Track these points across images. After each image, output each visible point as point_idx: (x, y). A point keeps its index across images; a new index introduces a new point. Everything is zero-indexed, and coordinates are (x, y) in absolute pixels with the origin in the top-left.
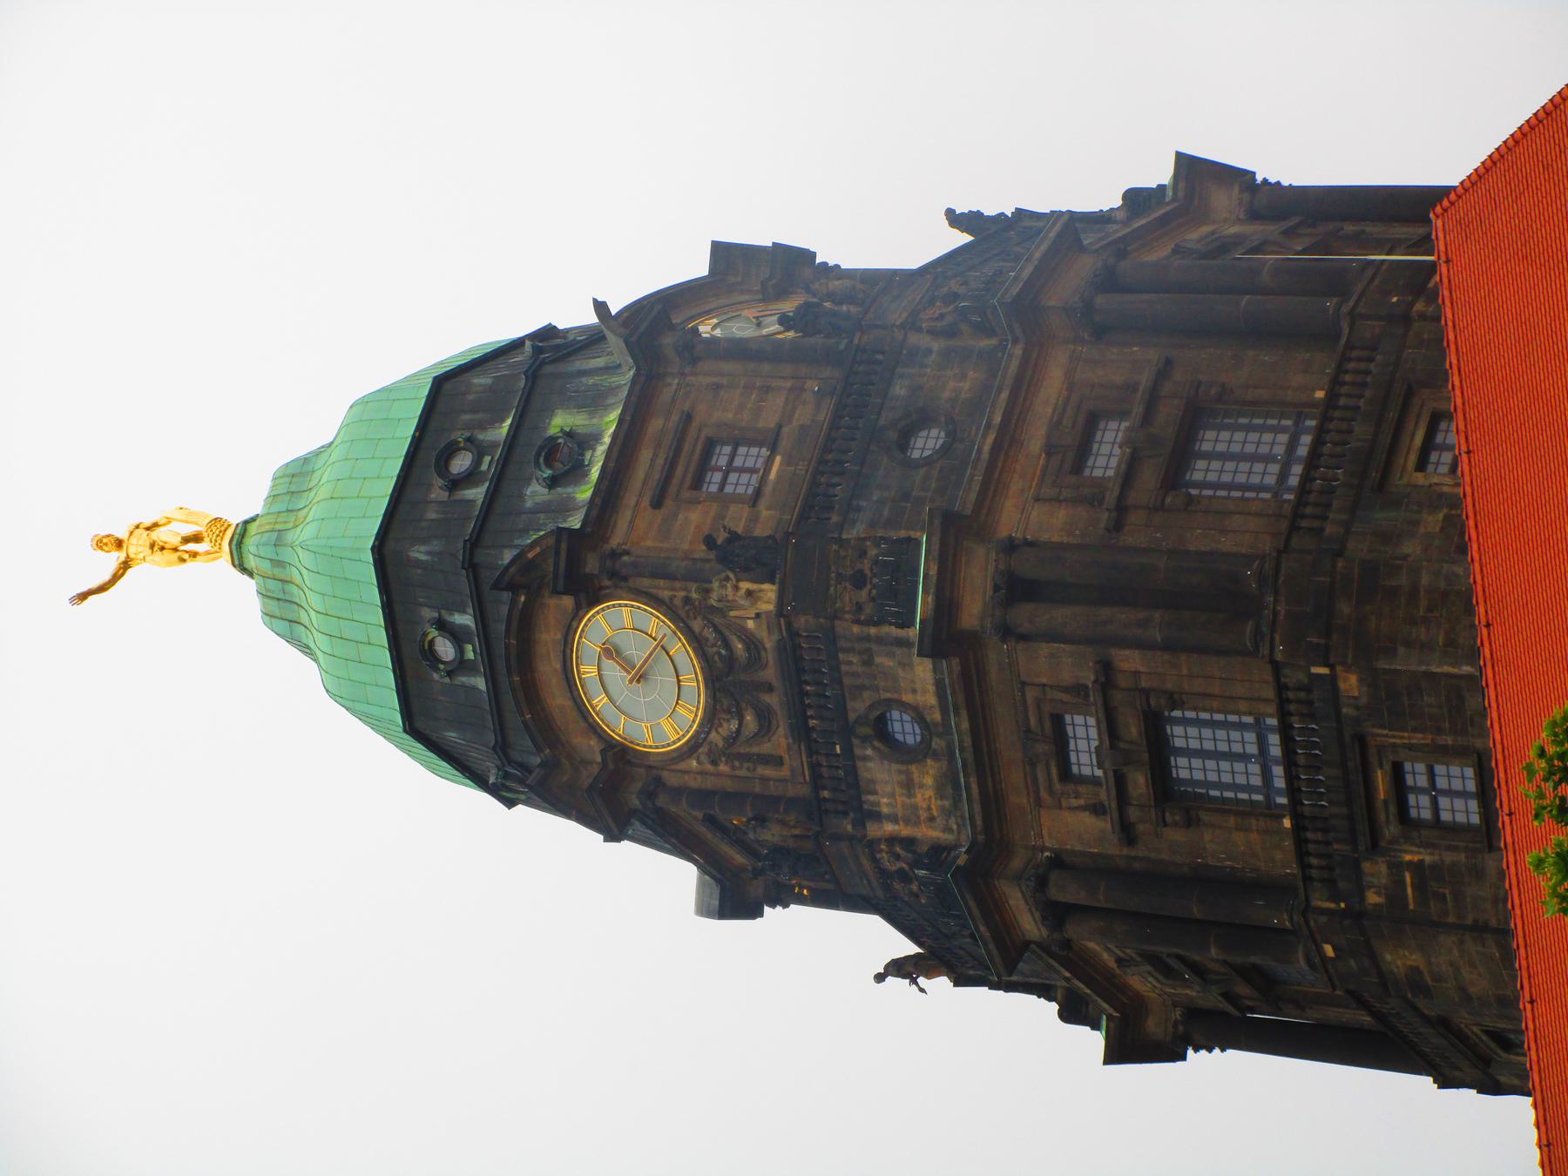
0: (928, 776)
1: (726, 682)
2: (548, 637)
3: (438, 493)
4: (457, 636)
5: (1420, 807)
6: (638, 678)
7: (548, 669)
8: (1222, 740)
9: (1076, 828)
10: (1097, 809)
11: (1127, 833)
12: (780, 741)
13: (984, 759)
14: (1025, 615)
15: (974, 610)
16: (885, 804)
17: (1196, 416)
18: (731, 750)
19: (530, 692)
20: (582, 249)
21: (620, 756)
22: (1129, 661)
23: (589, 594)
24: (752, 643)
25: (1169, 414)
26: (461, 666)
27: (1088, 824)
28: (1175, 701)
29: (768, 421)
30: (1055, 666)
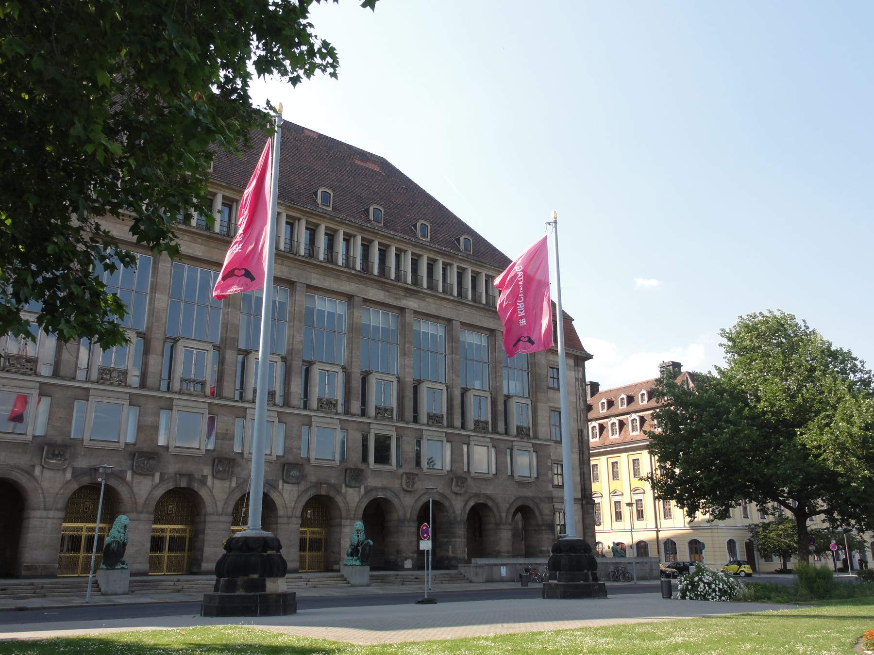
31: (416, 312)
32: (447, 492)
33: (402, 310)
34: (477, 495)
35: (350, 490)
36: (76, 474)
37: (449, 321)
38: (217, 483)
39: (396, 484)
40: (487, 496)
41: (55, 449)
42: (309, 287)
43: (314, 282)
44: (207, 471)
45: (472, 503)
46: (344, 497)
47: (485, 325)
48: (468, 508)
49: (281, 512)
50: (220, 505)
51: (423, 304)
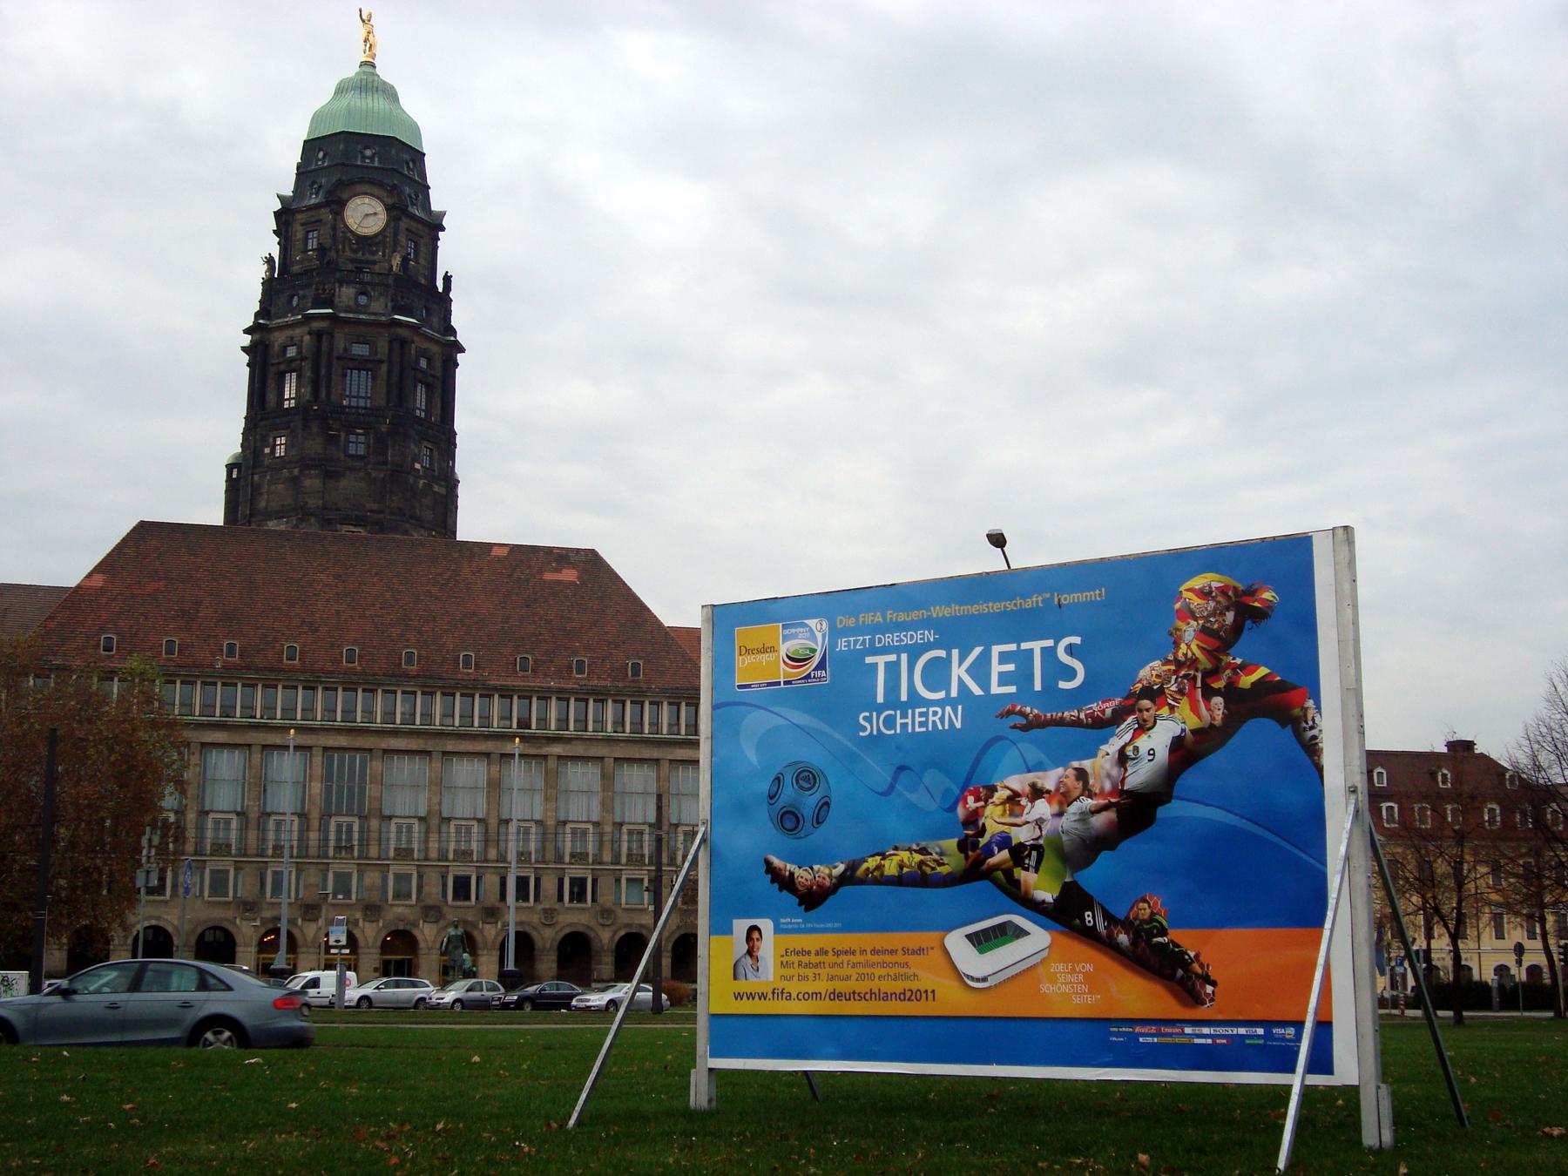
0: (352, 303)
1: (365, 242)
2: (375, 190)
3: (406, 157)
4: (372, 158)
5: (352, 438)
6: (365, 215)
7: (366, 188)
8: (363, 387)
9: (340, 345)
10: (345, 350)
11: (339, 358)
12: (349, 254)
13: (359, 322)
14: (396, 345)
15: (401, 332)
16: (344, 289)
17: (429, 387)
18: (345, 237)
19: (362, 181)
20: (445, 190)
21: (342, 204)
22: (384, 368)
23: (389, 209)
24: (374, 253)
25: (430, 380)
26: (364, 157)
27: (342, 346)
28: (373, 378)
29: (422, 261)
30: (383, 346)
31: (560, 757)
32: (593, 924)
33: (545, 757)
34: (627, 925)
35: (487, 926)
36: (264, 922)
37: (602, 758)
38: (367, 925)
39: (535, 918)
40: (641, 926)
41: (249, 907)
42: (445, 753)
43: (450, 748)
44: (358, 915)
45: (622, 933)
46: (481, 931)
47: (647, 756)
48: (617, 938)
49: (422, 945)
50: (370, 941)
51: (568, 747)
